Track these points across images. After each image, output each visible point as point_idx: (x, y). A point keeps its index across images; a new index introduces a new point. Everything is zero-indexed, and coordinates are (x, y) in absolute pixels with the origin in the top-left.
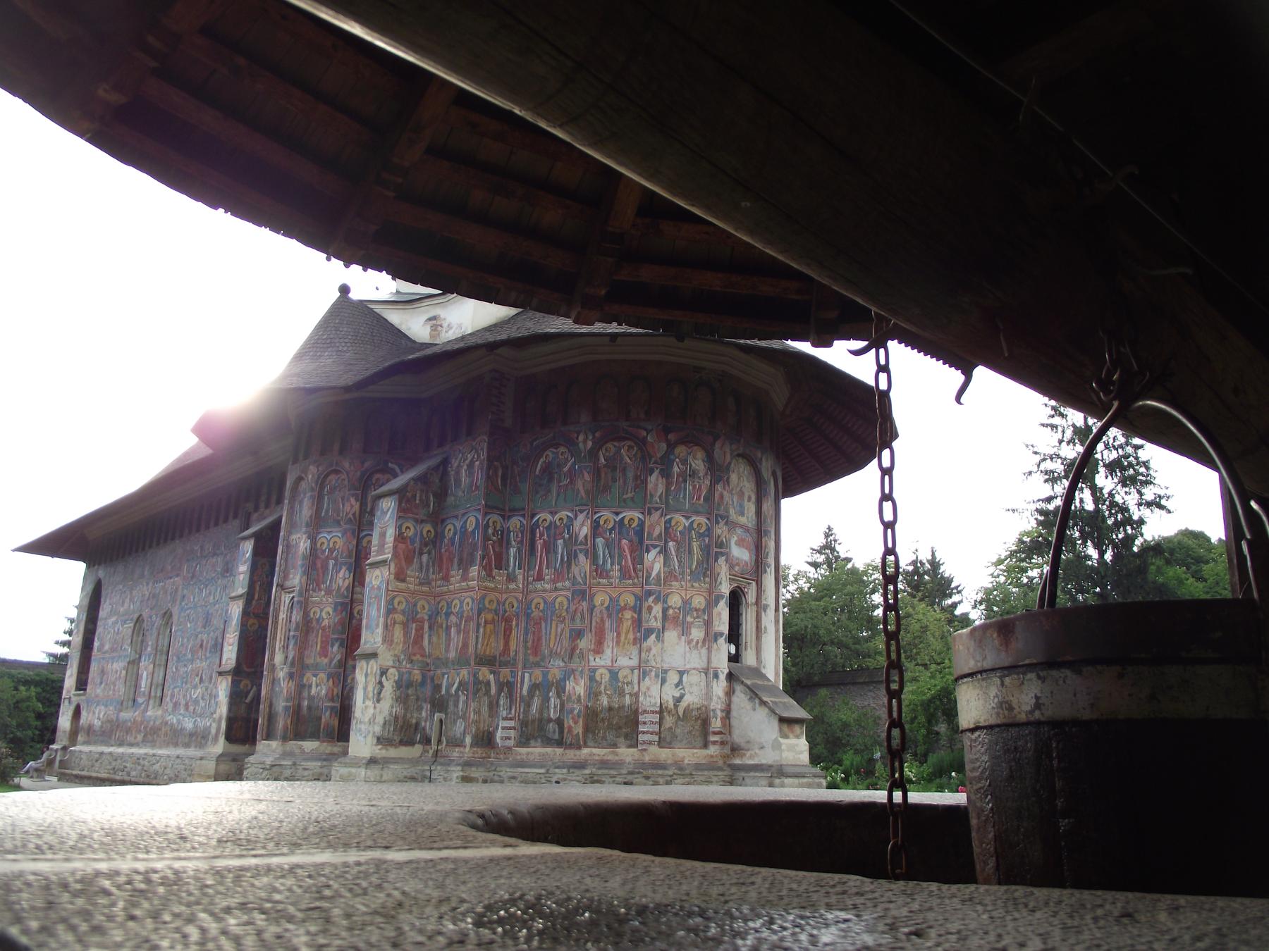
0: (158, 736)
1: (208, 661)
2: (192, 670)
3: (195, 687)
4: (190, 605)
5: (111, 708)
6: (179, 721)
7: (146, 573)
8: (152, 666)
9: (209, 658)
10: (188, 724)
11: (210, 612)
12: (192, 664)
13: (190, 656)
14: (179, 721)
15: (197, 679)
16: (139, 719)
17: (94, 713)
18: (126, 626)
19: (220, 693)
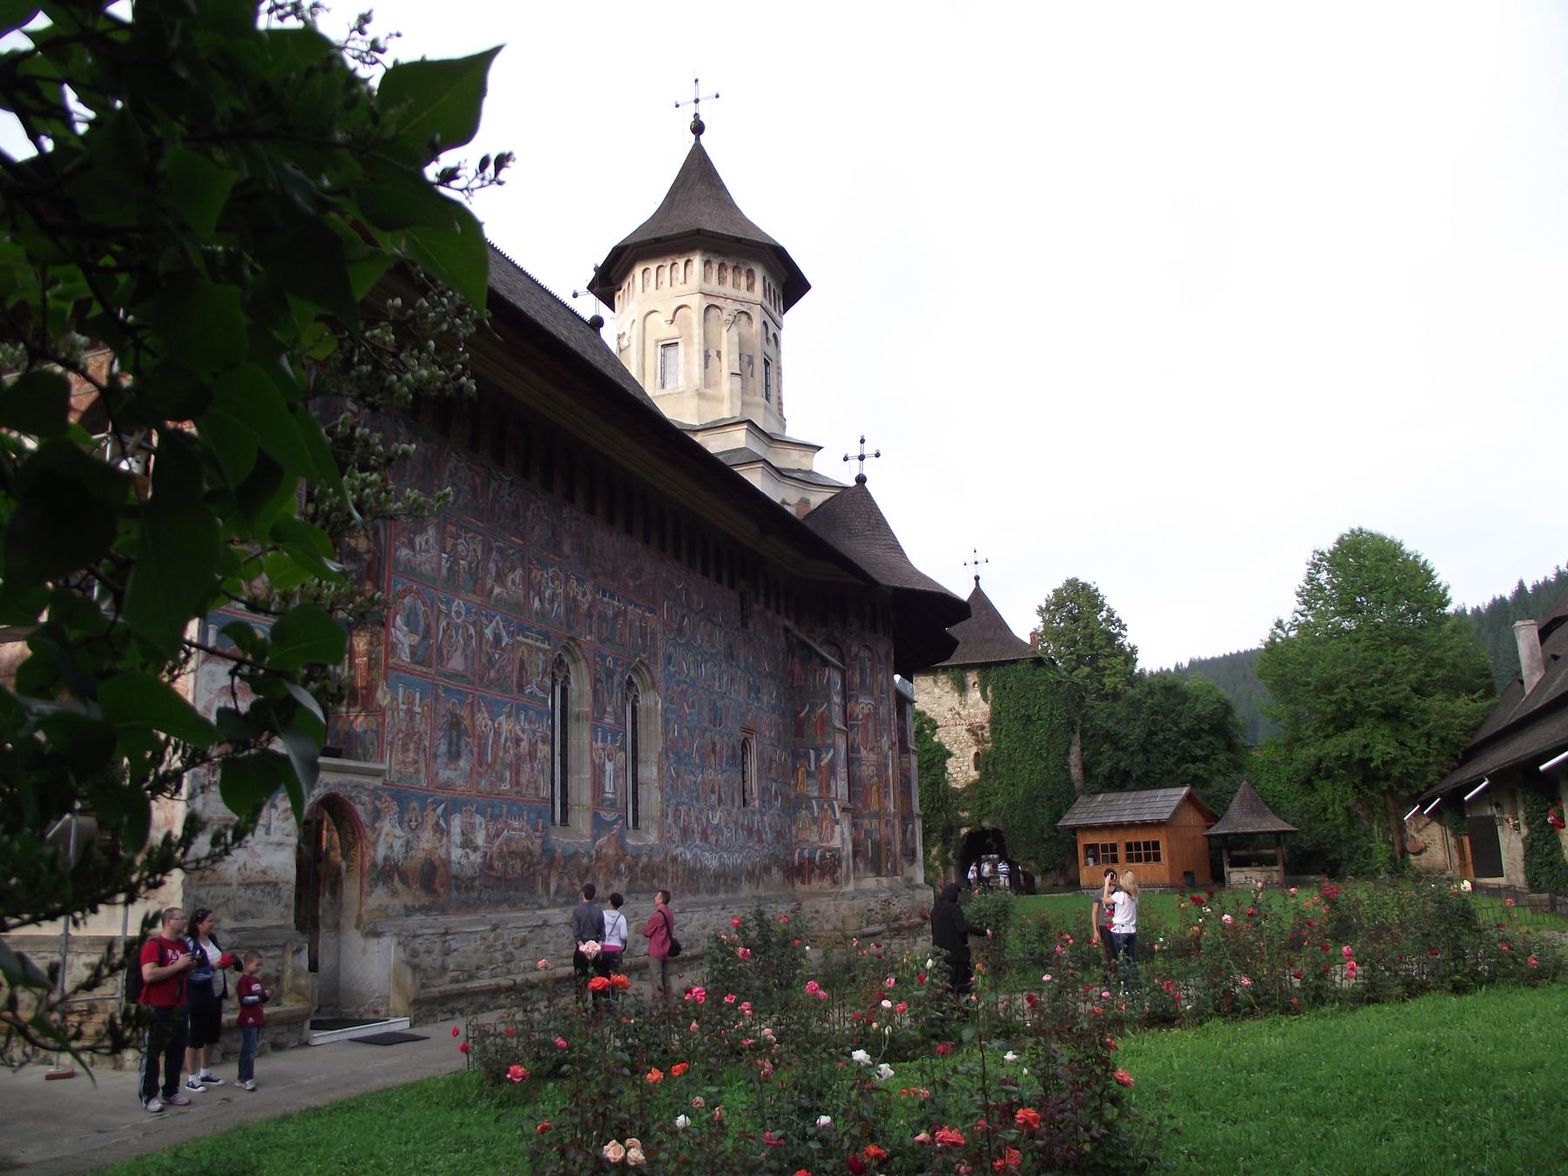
1: (725, 775)
2: (703, 782)
3: (712, 808)
4: (683, 677)
5: (516, 824)
6: (695, 855)
7: (566, 548)
9: (726, 771)
10: (711, 861)
13: (697, 760)
14: (695, 855)
15: (714, 798)
16: (611, 852)
17: (441, 831)
18: (520, 638)
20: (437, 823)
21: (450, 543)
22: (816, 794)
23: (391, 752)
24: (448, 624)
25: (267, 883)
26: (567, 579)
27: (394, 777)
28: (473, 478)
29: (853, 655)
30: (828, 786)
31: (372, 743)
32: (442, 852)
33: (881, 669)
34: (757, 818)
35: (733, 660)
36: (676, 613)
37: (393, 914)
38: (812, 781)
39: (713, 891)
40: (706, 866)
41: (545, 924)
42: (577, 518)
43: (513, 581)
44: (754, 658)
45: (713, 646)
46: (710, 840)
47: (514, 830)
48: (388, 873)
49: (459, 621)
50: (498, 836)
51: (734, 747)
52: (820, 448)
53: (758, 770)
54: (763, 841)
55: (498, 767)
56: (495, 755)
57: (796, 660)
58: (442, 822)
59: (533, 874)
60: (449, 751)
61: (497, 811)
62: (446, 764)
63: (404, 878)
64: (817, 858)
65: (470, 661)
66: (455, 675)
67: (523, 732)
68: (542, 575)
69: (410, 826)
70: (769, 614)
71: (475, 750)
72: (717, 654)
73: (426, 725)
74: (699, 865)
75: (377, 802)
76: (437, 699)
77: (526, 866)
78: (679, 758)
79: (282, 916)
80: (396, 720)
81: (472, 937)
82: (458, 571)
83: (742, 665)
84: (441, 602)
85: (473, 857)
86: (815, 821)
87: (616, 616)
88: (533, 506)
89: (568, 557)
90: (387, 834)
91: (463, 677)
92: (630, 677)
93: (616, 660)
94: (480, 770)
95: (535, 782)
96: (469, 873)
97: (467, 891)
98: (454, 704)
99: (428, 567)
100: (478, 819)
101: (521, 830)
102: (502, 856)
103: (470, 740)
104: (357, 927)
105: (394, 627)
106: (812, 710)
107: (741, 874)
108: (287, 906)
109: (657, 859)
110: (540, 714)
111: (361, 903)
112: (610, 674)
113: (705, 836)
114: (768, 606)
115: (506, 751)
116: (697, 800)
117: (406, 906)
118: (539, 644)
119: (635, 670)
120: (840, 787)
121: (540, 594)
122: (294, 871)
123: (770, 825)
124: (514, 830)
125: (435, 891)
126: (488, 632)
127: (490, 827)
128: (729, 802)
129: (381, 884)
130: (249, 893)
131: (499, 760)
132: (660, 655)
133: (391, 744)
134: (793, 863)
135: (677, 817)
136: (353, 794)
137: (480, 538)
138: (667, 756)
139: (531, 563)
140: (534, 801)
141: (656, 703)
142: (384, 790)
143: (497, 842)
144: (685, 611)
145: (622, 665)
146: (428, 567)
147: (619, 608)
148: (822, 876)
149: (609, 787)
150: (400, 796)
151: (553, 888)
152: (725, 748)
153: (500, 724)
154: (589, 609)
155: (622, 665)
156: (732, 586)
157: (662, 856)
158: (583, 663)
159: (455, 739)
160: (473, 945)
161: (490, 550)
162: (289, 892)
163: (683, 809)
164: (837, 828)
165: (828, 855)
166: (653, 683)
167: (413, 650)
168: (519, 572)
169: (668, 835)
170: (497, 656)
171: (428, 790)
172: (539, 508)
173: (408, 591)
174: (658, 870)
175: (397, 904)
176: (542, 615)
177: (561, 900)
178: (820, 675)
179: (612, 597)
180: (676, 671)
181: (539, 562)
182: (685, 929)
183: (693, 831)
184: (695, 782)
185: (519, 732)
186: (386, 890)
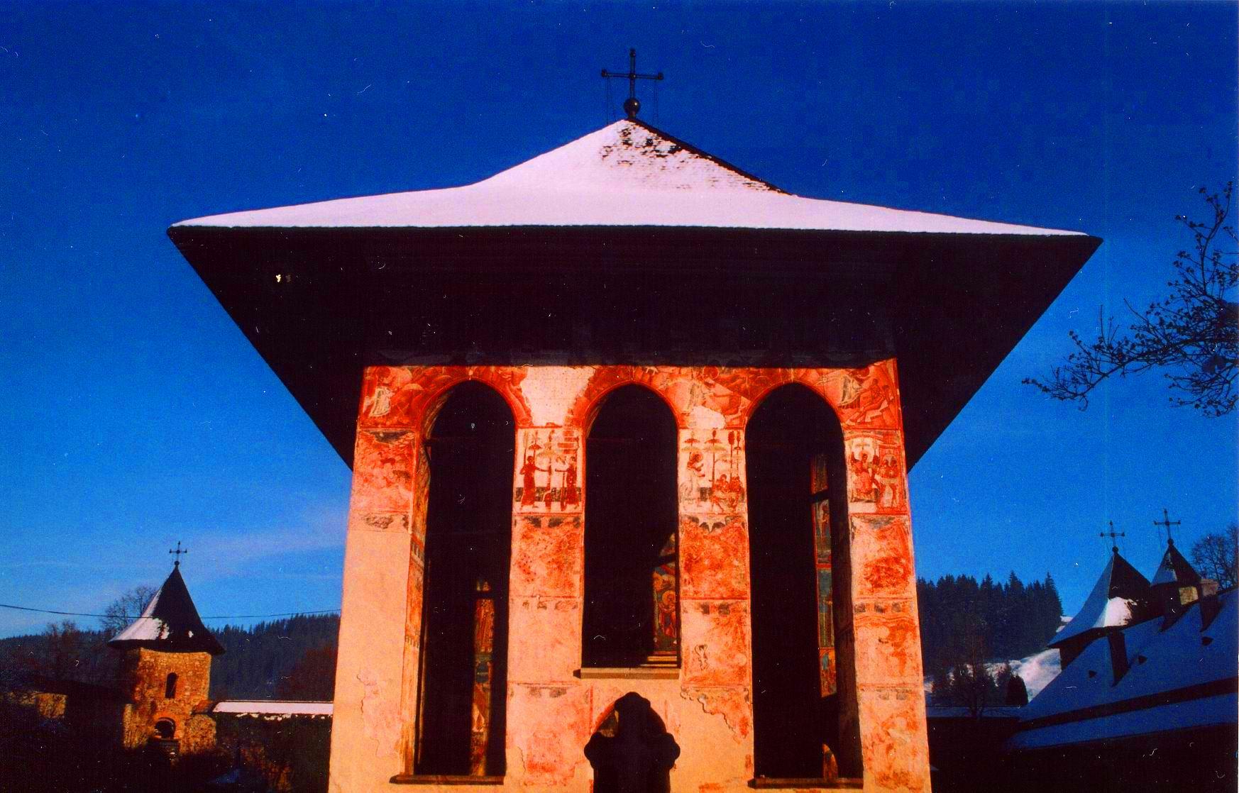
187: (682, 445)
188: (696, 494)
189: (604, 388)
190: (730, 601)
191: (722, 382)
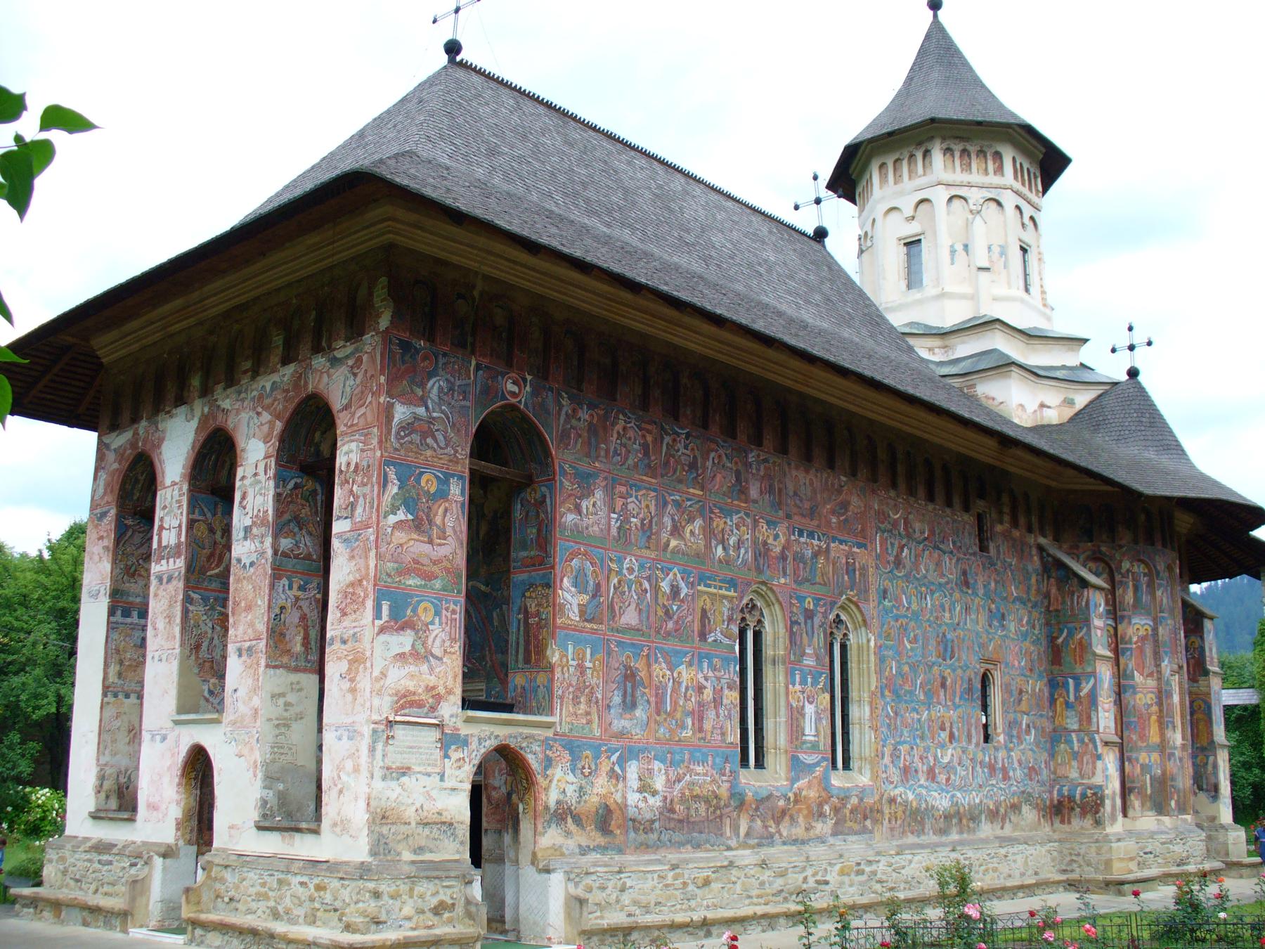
0: (875, 821)
1: (959, 710)
2: (930, 719)
3: (942, 746)
4: (903, 611)
5: (699, 769)
7: (754, 492)
8: (827, 696)
9: (959, 706)
10: (942, 802)
11: (949, 636)
12: (929, 709)
15: (944, 735)
16: (813, 794)
18: (701, 588)
19: (1109, 766)
20: (612, 770)
21: (619, 503)
22: (1076, 727)
23: (561, 705)
24: (619, 582)
25: (444, 823)
26: (756, 523)
27: (565, 728)
28: (644, 436)
29: (1123, 571)
30: (1089, 718)
31: (544, 698)
32: (619, 799)
33: (1160, 586)
34: (1001, 754)
35: (968, 588)
36: (892, 544)
37: (567, 852)
38: (1071, 713)
39: (943, 832)
40: (933, 807)
41: (731, 864)
42: (765, 461)
43: (692, 533)
44: (997, 582)
45: (942, 575)
46: (939, 780)
47: (699, 774)
48: (562, 814)
49: (632, 577)
50: (679, 781)
51: (970, 680)
52: (1085, 341)
53: (1003, 703)
54: (1009, 778)
55: (678, 715)
56: (675, 704)
57: (1052, 580)
58: (617, 768)
59: (721, 817)
60: (624, 701)
61: (677, 757)
62: (621, 715)
63: (578, 820)
64: (1078, 797)
65: (644, 615)
66: (629, 629)
67: (706, 679)
68: (725, 523)
69: (582, 773)
70: (1016, 533)
71: (653, 699)
72: (947, 583)
73: (598, 679)
74: (924, 806)
75: (547, 752)
76: (609, 654)
77: (711, 809)
78: (897, 696)
79: (458, 852)
80: (566, 675)
81: (649, 876)
82: (630, 529)
83: (981, 592)
84: (611, 560)
85: (651, 800)
86: (1076, 756)
87: (816, 555)
88: (713, 455)
89: (755, 502)
90: (559, 781)
91: (638, 630)
92: (838, 616)
93: (817, 601)
94: (658, 718)
95: (721, 728)
96: (648, 816)
97: (646, 833)
98: (628, 657)
99: (596, 528)
100: (657, 765)
101: (706, 775)
102: (683, 799)
103: (647, 690)
104: (533, 863)
105: (561, 588)
106: (1070, 635)
107: (981, 813)
108: (462, 843)
109: (869, 800)
110: (726, 661)
111: (535, 842)
112: (809, 615)
113: (931, 775)
114: (1015, 523)
115: (686, 699)
116: (922, 738)
117: (580, 846)
118: (723, 592)
119: (842, 608)
120: (1105, 719)
121: (723, 542)
122: (468, 813)
123: (1020, 763)
124: (699, 774)
125: (612, 832)
126: (665, 586)
127: (671, 773)
128: (964, 738)
129: (554, 826)
130: (427, 831)
131: (680, 709)
132: (873, 589)
133: (562, 698)
134: (1052, 800)
135: (895, 756)
136: (524, 745)
137: (653, 494)
138: (883, 695)
139: (711, 512)
140: (720, 747)
141: (869, 641)
142: (555, 740)
143: (678, 787)
144: (904, 541)
145: (825, 605)
146: (596, 528)
147: (820, 547)
148: (1084, 814)
149: (809, 729)
150: (573, 747)
151: (743, 831)
152: (959, 683)
153: (679, 673)
154: (783, 552)
155: (825, 605)
156: (966, 509)
157: (877, 797)
158: (777, 607)
159: (629, 690)
160: (650, 884)
161: (665, 504)
162: (464, 831)
163: (903, 748)
164: (1099, 763)
165: (1089, 792)
166: (864, 621)
167: (582, 610)
168: (698, 522)
169: (884, 776)
170: (675, 608)
171: (601, 739)
172: (720, 456)
173: (574, 554)
174: (871, 811)
175: (571, 844)
176: (727, 562)
177: (753, 842)
178: (1078, 597)
179: (811, 535)
180: (894, 606)
181: (720, 509)
182: (903, 871)
183: (916, 771)
184: (919, 720)
185: (702, 680)
186: (559, 831)
187: (238, 484)
188: (242, 534)
189: (201, 439)
190: (254, 642)
191: (266, 408)
